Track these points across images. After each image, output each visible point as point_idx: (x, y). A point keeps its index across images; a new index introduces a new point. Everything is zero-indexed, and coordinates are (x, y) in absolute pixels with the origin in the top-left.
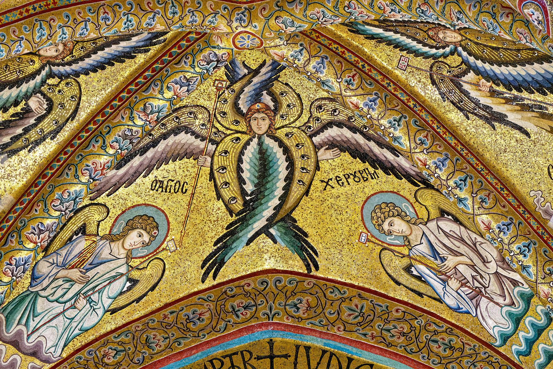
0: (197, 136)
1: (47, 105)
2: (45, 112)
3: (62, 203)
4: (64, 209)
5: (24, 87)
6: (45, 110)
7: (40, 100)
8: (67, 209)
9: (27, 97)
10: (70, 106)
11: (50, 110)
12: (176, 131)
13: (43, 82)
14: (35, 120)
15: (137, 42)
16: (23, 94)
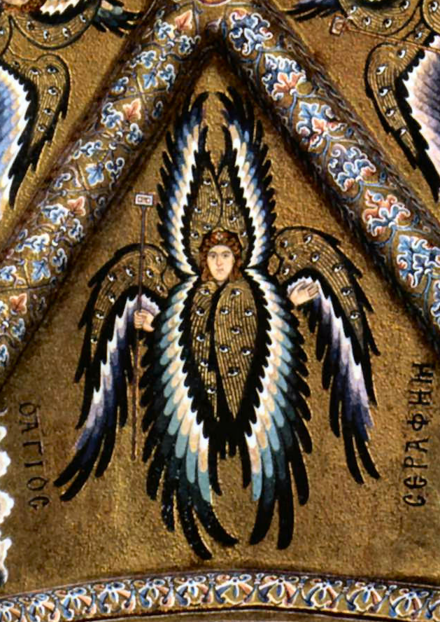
0: (414, 63)
1: (307, 277)
2: (317, 282)
3: (413, 272)
4: (421, 269)
5: (272, 307)
6: (314, 280)
7: (299, 287)
8: (423, 266)
9: (286, 305)
10: (315, 242)
11: (316, 275)
12: (401, 93)
13: (270, 279)
14: (326, 297)
15: (242, 140)
16: (282, 310)
